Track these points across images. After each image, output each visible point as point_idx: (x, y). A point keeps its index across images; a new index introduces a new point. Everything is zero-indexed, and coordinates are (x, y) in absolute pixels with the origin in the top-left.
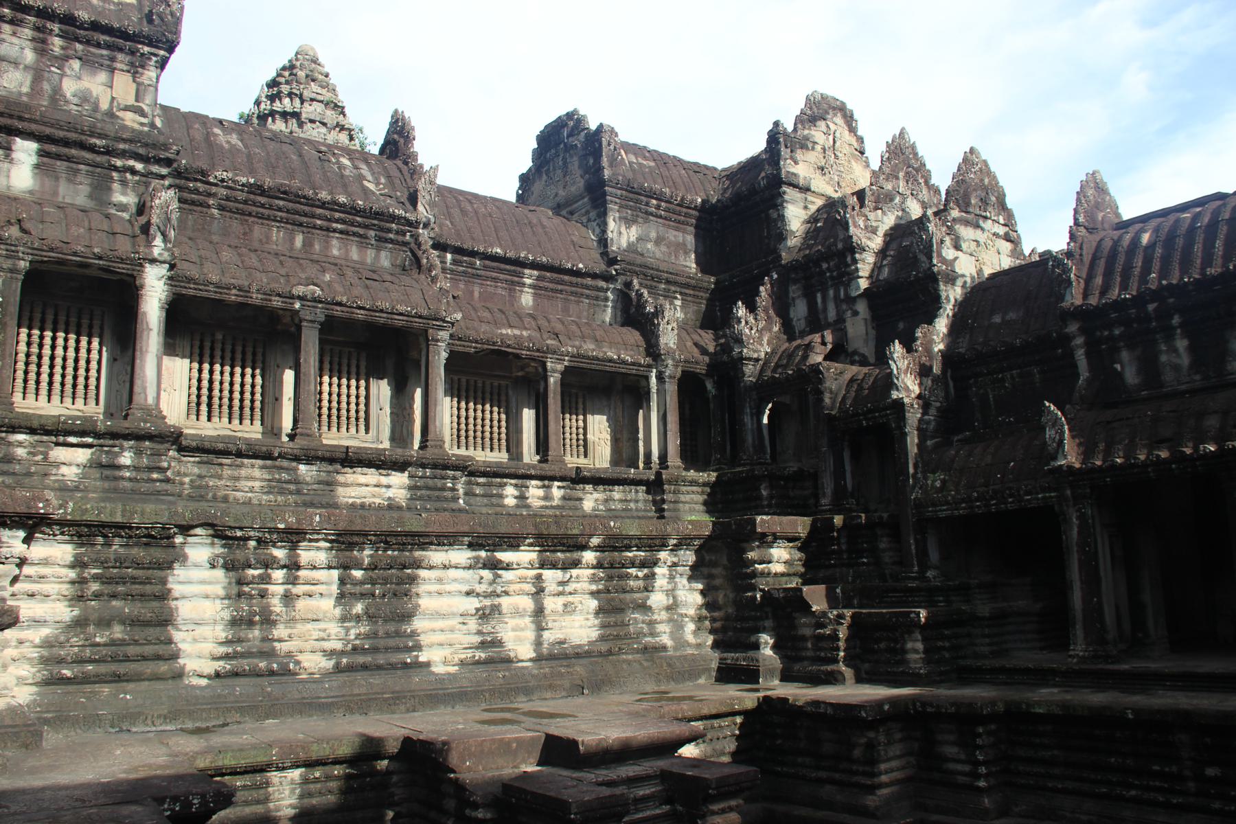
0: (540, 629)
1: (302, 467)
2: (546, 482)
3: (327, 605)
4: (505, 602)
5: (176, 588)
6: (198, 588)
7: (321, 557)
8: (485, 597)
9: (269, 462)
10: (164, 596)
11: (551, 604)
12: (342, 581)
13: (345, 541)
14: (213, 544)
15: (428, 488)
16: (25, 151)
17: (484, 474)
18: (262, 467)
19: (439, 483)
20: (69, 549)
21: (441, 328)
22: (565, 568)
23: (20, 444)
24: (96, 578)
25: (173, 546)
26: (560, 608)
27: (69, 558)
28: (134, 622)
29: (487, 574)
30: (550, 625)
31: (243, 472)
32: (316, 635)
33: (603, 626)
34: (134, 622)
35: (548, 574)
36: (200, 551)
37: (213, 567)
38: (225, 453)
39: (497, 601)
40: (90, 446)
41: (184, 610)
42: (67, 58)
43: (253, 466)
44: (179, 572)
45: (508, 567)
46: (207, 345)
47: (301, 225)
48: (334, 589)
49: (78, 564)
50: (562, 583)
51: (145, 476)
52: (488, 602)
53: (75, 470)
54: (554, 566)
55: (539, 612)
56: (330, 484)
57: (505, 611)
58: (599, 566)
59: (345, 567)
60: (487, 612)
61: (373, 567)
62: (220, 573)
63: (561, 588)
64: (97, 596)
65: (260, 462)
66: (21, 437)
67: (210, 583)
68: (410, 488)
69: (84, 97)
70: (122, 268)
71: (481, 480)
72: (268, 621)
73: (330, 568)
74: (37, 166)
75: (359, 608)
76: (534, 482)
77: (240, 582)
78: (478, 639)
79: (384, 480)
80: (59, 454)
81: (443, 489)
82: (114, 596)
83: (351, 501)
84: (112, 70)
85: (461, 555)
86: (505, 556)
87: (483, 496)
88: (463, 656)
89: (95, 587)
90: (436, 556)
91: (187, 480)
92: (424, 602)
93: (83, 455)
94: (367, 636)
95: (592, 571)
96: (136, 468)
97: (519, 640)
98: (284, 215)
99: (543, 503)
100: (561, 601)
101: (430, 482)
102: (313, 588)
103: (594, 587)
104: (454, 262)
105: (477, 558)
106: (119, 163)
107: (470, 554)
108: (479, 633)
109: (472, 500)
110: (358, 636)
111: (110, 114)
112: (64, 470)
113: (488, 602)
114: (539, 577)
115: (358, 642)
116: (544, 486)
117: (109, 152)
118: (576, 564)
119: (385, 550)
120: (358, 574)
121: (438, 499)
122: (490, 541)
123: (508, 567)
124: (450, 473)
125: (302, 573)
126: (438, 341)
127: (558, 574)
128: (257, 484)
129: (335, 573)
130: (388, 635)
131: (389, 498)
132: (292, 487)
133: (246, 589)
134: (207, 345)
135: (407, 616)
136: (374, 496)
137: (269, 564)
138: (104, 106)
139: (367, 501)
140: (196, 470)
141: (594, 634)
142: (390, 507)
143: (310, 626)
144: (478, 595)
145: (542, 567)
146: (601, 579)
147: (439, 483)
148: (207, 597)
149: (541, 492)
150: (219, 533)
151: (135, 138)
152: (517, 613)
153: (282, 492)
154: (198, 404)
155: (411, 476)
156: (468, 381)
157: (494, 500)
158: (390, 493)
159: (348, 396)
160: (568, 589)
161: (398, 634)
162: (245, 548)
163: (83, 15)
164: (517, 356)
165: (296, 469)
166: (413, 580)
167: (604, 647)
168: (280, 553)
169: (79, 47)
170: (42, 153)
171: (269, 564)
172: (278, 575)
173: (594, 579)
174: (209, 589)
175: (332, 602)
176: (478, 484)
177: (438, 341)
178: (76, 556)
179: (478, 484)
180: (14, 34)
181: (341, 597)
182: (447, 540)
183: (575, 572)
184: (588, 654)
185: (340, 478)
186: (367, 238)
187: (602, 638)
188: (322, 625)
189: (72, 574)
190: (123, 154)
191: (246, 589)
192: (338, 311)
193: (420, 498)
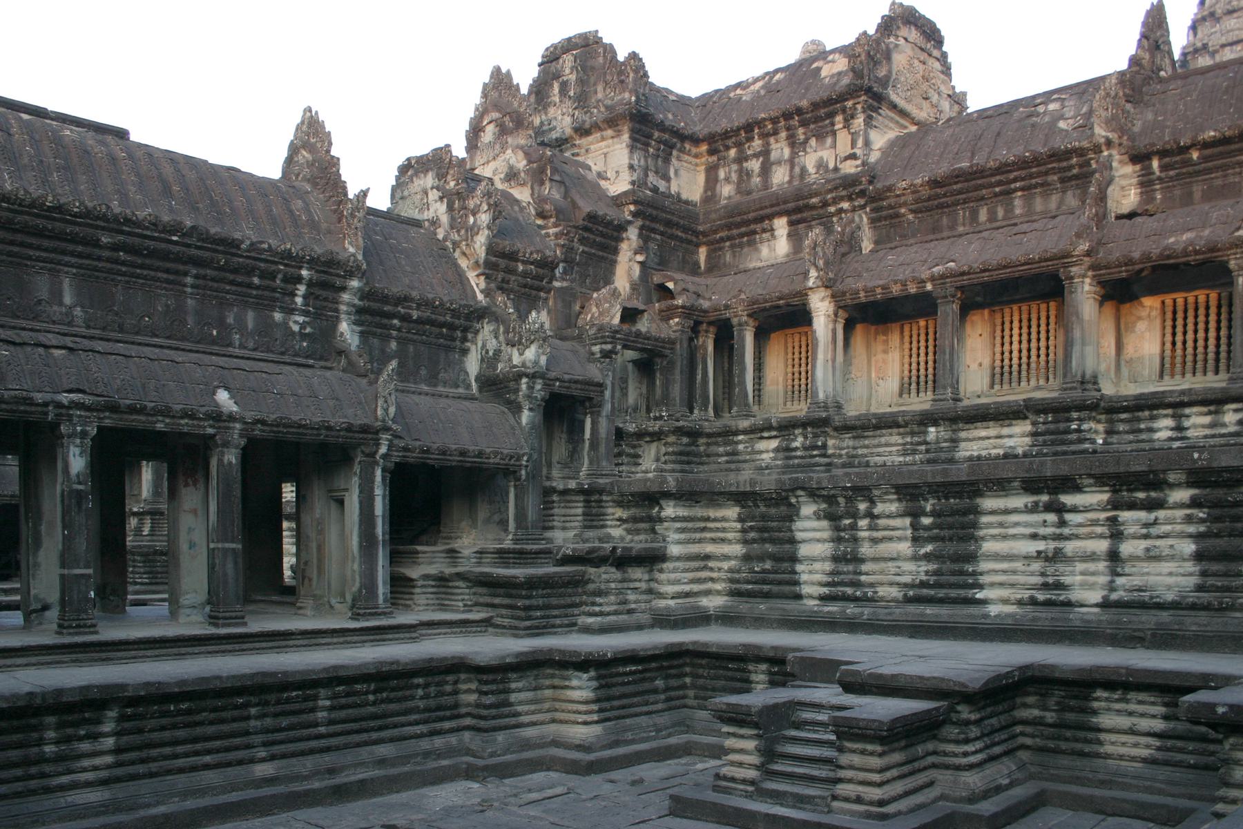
0: (1115, 574)
1: (932, 429)
2: (1212, 408)
3: (905, 547)
4: (1070, 547)
5: (799, 536)
6: (813, 536)
7: (893, 507)
8: (1054, 539)
9: (901, 430)
10: (793, 541)
11: (1127, 548)
12: (915, 526)
13: (909, 493)
14: (815, 502)
15: (1052, 433)
16: (781, 225)
17: (1126, 409)
18: (899, 434)
19: (1062, 426)
20: (737, 509)
21: (1074, 264)
22: (1151, 506)
23: (740, 442)
24: (752, 528)
25: (791, 505)
26: (1140, 553)
27: (735, 516)
28: (776, 558)
29: (1051, 517)
30: (1127, 570)
31: (883, 440)
32: (893, 570)
33: (1204, 574)
34: (776, 558)
35: (1125, 515)
36: (808, 509)
37: (819, 518)
38: (864, 428)
39: (1060, 544)
40: (775, 437)
41: (804, 550)
42: (806, 141)
43: (891, 435)
44: (799, 524)
45: (1074, 510)
46: (915, 333)
47: (983, 198)
48: (909, 532)
49: (740, 519)
50: (1146, 525)
51: (807, 453)
52: (1052, 545)
53: (772, 455)
54: (1132, 506)
55: (1113, 556)
56: (955, 441)
57: (1070, 554)
58: (1195, 503)
59: (915, 514)
60: (1050, 555)
61: (933, 513)
62: (825, 523)
63: (1144, 531)
64: (754, 541)
65: (895, 430)
66: (741, 437)
67: (819, 530)
68: (1034, 434)
69: (821, 165)
70: (795, 301)
71: (1124, 416)
72: (859, 560)
73: (901, 516)
74: (789, 235)
75: (929, 548)
76: (1195, 409)
77: (838, 529)
78: (1038, 580)
79: (1005, 431)
80: (762, 445)
81: (1068, 431)
82: (764, 541)
83: (968, 454)
84: (834, 133)
85: (1019, 501)
86: (1068, 499)
87: (1127, 432)
88: (1019, 596)
89: (752, 535)
90: (988, 503)
91: (844, 452)
92: (988, 546)
93: (774, 444)
94: (936, 573)
95: (1188, 511)
96: (805, 448)
97: (1091, 586)
98: (964, 196)
99: (1208, 432)
100: (1144, 544)
101: (1052, 426)
102: (892, 533)
103: (1192, 529)
104: (1163, 168)
105: (1036, 504)
106: (832, 209)
107: (1029, 499)
108: (1043, 574)
109: (1115, 439)
110: (927, 573)
111: (836, 169)
112: (764, 456)
113: (1052, 545)
114: (1113, 521)
115: (924, 578)
116: (1210, 413)
117: (825, 204)
118: (1159, 505)
119: (947, 498)
120: (926, 521)
121: (1063, 443)
122: (1048, 485)
123: (1074, 510)
124: (1075, 415)
125: (882, 522)
126: (1072, 278)
127: (1142, 515)
128: (894, 449)
129: (908, 521)
130: (953, 573)
131: (1010, 447)
132: (923, 448)
133: (843, 534)
134: (915, 333)
135: (972, 558)
136: (995, 447)
137: (855, 515)
138: (831, 166)
139: (984, 453)
140: (851, 443)
141: (1193, 581)
142: (1006, 456)
143: (890, 564)
144: (1044, 538)
145: (1115, 508)
146: (1202, 521)
147: (1062, 426)
148: (818, 540)
149: (1207, 420)
150: (814, 494)
151: (849, 183)
152: (1091, 557)
153: (914, 452)
154: (910, 384)
155: (1034, 424)
156: (1186, 299)
157: (1144, 436)
158: (1010, 442)
159: (1039, 349)
160: (1154, 531)
161: (962, 573)
162: (845, 503)
163: (804, 103)
164: (1187, 264)
165: (926, 433)
166: (975, 525)
167: (1192, 597)
168: (862, 506)
169: (812, 126)
170: (791, 223)
171: (855, 515)
172: (863, 523)
173: (1189, 519)
174: (818, 535)
175: (909, 544)
176: (1122, 421)
177: (1072, 278)
178: (739, 514)
179: (1122, 421)
180: (777, 141)
181: (915, 539)
182: (1001, 486)
183: (1161, 514)
184: (1174, 606)
185: (963, 435)
186: (1049, 185)
187: (1200, 588)
188: (900, 564)
189: (739, 526)
190: (835, 201)
191: (843, 534)
192: (965, 280)
193: (1045, 444)
